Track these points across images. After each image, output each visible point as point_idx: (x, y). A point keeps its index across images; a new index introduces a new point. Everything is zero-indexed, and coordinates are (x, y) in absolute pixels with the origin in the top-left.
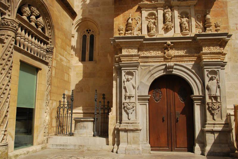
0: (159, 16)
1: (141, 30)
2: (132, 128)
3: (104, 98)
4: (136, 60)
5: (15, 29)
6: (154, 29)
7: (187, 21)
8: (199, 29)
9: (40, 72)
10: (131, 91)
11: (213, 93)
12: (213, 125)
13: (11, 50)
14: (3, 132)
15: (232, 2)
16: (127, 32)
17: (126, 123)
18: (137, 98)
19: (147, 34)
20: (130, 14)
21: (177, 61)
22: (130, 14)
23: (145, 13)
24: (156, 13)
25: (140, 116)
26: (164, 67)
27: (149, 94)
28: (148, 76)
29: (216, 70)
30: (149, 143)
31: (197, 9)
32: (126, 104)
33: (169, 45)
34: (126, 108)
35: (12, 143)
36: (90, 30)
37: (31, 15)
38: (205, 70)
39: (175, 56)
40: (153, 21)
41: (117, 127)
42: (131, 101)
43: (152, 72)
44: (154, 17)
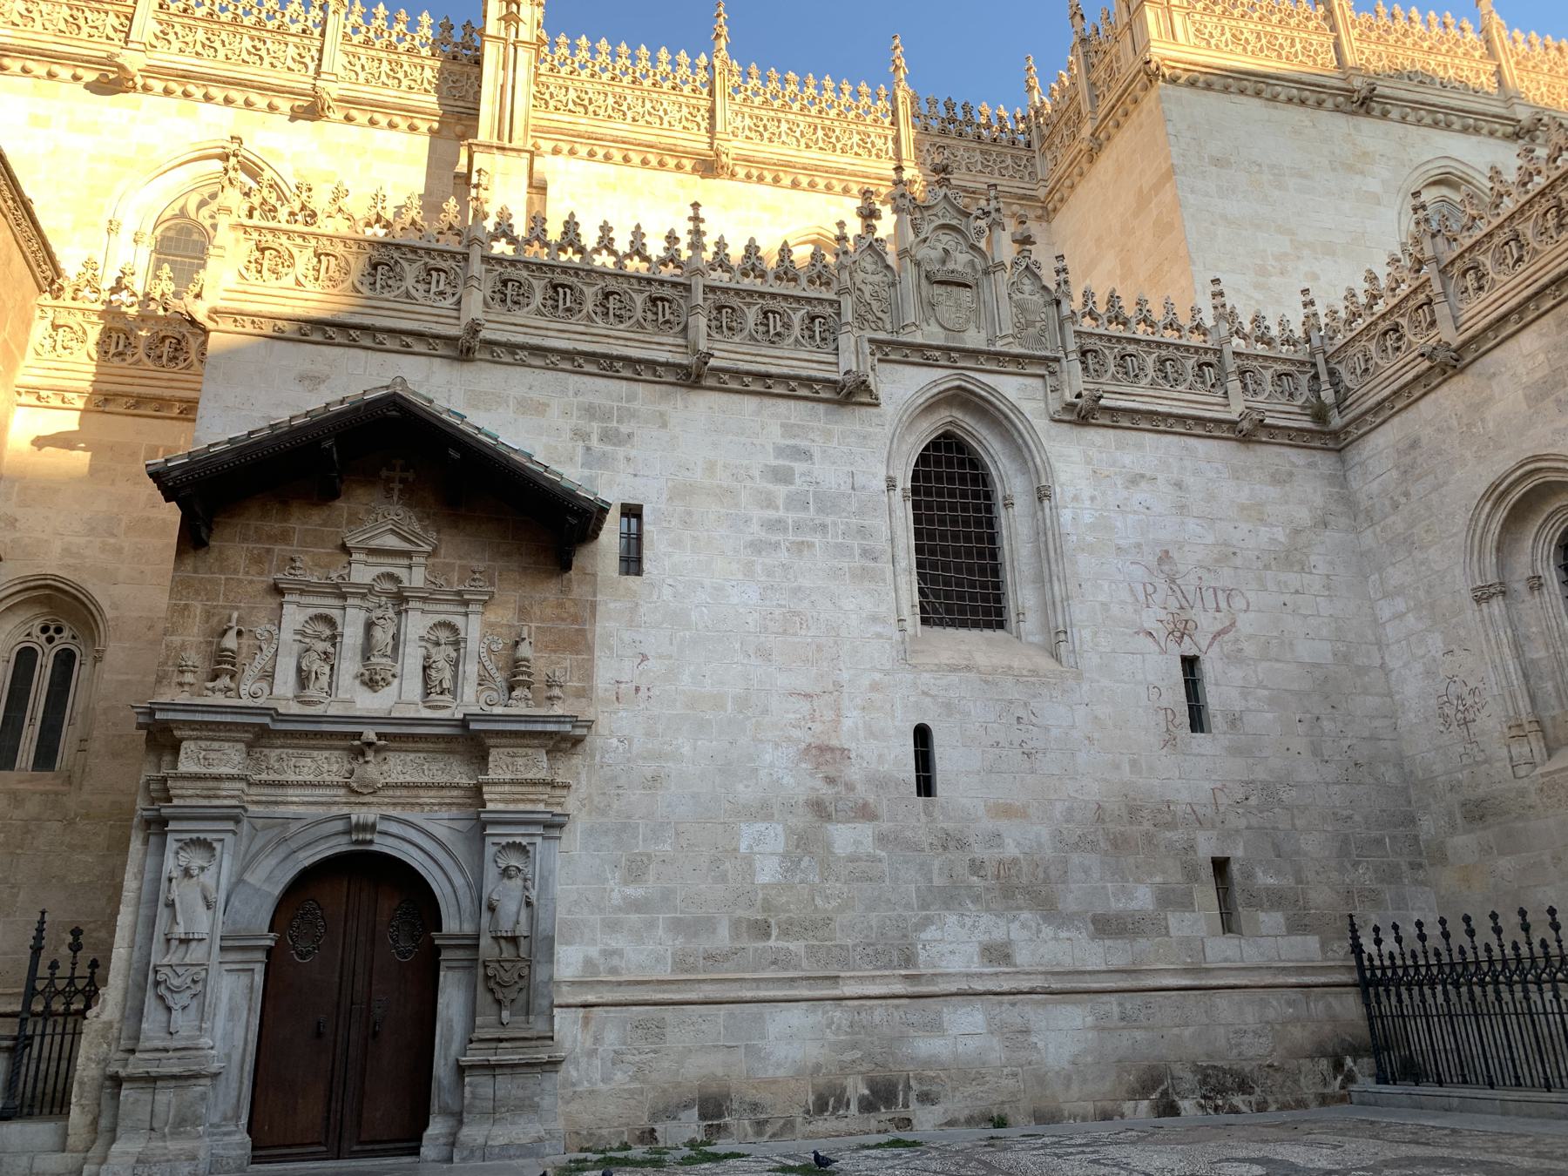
0: (348, 631)
1: (269, 676)
2: (176, 1070)
3: (76, 947)
4: (233, 797)
6: (324, 680)
7: (448, 660)
8: (487, 693)
11: (506, 927)
12: (493, 1045)
15: (612, 605)
16: (210, 685)
19: (290, 695)
20: (235, 615)
21: (395, 804)
22: (235, 615)
23: (295, 615)
24: (339, 621)
25: (223, 1019)
27: (271, 930)
28: (273, 861)
29: (524, 841)
30: (249, 1131)
31: (491, 617)
32: (164, 970)
33: (370, 744)
34: (162, 990)
36: (59, 630)
38: (489, 840)
39: (387, 786)
40: (321, 646)
41: (111, 1070)
42: (187, 960)
44: (328, 632)
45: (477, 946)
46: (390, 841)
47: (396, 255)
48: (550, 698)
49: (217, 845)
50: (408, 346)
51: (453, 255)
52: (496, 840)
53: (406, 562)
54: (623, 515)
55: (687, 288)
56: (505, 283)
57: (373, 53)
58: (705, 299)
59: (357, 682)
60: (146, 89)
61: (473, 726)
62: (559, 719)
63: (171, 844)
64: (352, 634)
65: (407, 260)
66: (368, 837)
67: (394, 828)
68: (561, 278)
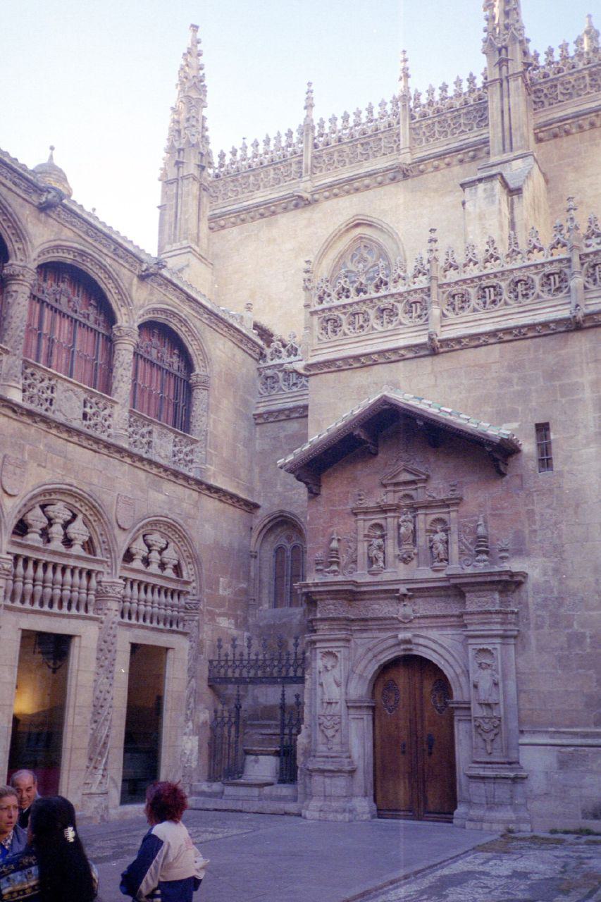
2: (331, 768)
5: (119, 596)
9: (170, 654)
10: (335, 693)
13: (111, 632)
14: (101, 772)
17: (324, 757)
18: (344, 704)
26: (392, 642)
29: (490, 647)
32: (322, 718)
33: (405, 595)
34: (322, 728)
35: (115, 794)
37: (150, 551)
38: (470, 648)
43: (376, 651)
44: (379, 533)
45: (469, 709)
46: (420, 648)
47: (392, 301)
48: (502, 558)
49: (338, 655)
50: (403, 355)
51: (422, 290)
52: (475, 647)
53: (413, 487)
54: (537, 430)
55: (569, 260)
56: (453, 296)
57: (430, 122)
58: (582, 264)
59: (397, 561)
60: (316, 201)
61: (453, 581)
62: (500, 573)
63: (319, 656)
64: (391, 533)
65: (398, 302)
66: (409, 646)
67: (421, 641)
68: (485, 283)
